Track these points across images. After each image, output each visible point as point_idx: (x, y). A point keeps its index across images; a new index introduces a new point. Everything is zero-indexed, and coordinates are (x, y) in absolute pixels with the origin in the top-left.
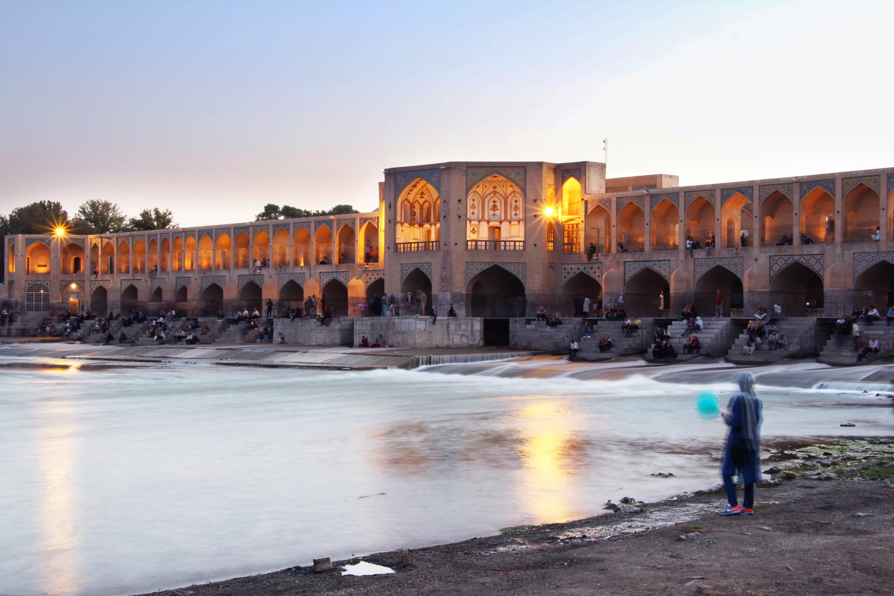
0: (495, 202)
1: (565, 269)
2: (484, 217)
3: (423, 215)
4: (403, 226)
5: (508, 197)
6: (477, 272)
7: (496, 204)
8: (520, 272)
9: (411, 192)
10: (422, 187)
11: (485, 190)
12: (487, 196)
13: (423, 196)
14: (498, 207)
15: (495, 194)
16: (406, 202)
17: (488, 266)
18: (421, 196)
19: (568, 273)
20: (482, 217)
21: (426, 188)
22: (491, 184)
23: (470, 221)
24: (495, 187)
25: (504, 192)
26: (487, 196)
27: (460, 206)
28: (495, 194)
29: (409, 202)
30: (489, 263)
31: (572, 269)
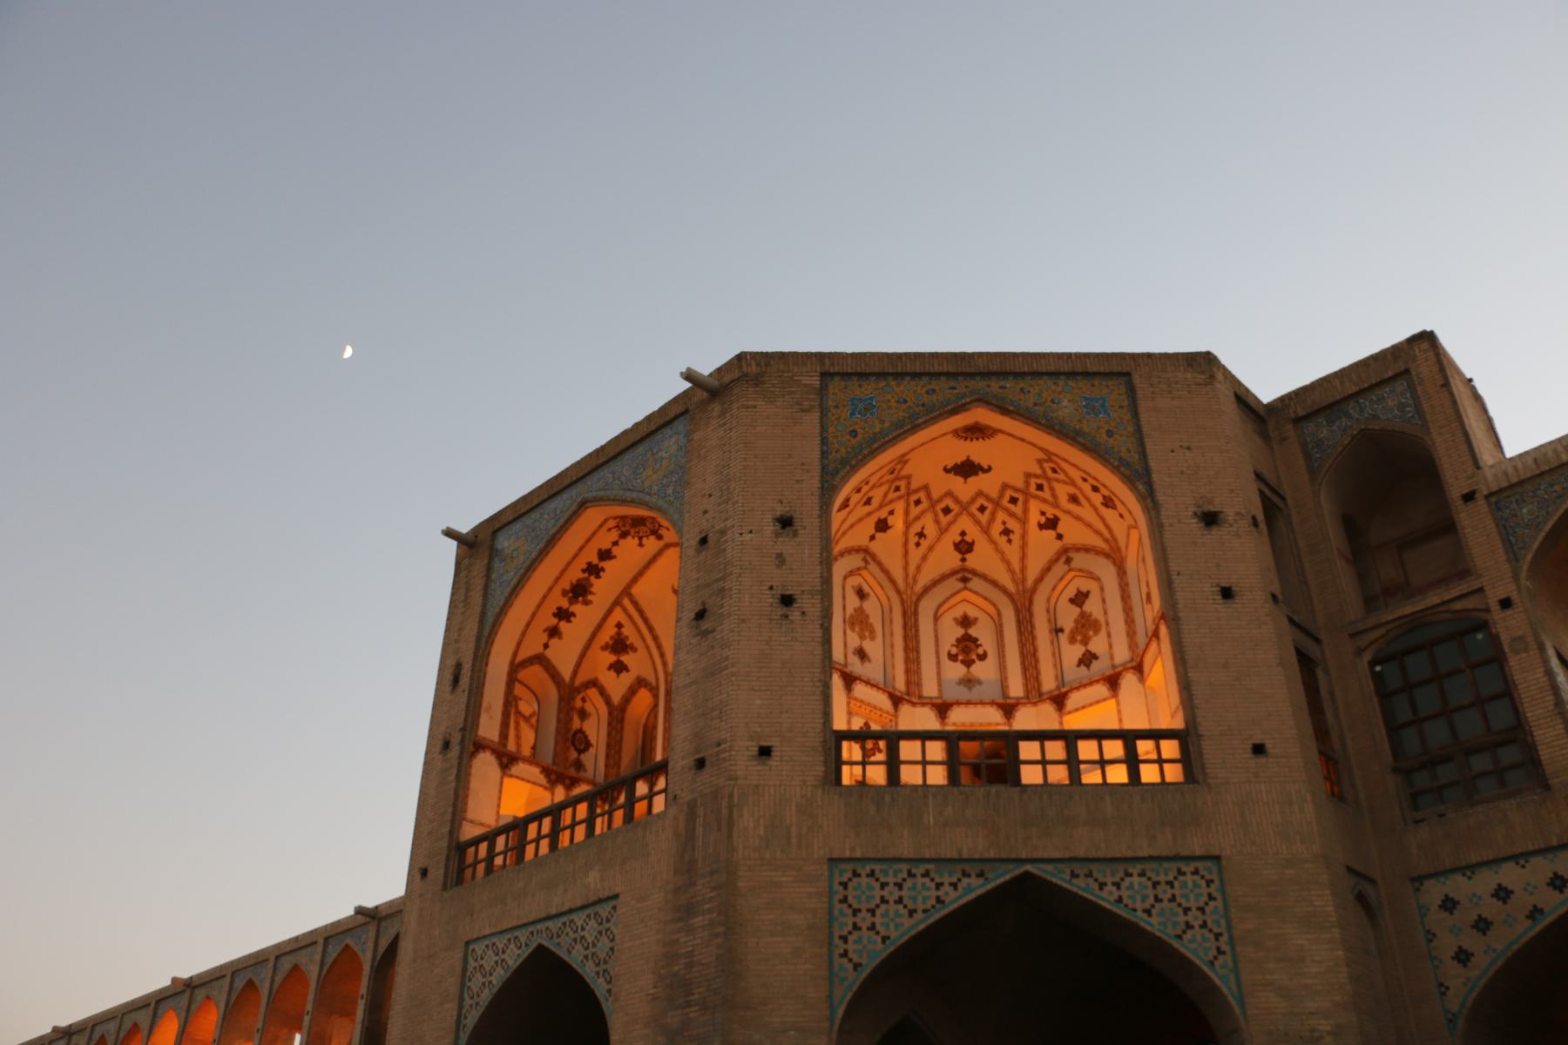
0: (966, 622)
1: (1449, 904)
2: (919, 685)
3: (619, 752)
4: (515, 770)
5: (1034, 591)
6: (907, 922)
7: (973, 632)
8: (1195, 918)
9: (563, 625)
10: (617, 602)
11: (915, 555)
12: (926, 590)
13: (625, 659)
14: (986, 639)
15: (965, 580)
16: (535, 674)
17: (975, 888)
18: (612, 658)
19: (1482, 925)
20: (908, 683)
21: (635, 604)
22: (944, 520)
23: (849, 680)
24: (964, 547)
25: (1011, 571)
26: (926, 590)
27: (787, 545)
28: (965, 580)
29: (554, 674)
30: (981, 865)
31: (1502, 894)
